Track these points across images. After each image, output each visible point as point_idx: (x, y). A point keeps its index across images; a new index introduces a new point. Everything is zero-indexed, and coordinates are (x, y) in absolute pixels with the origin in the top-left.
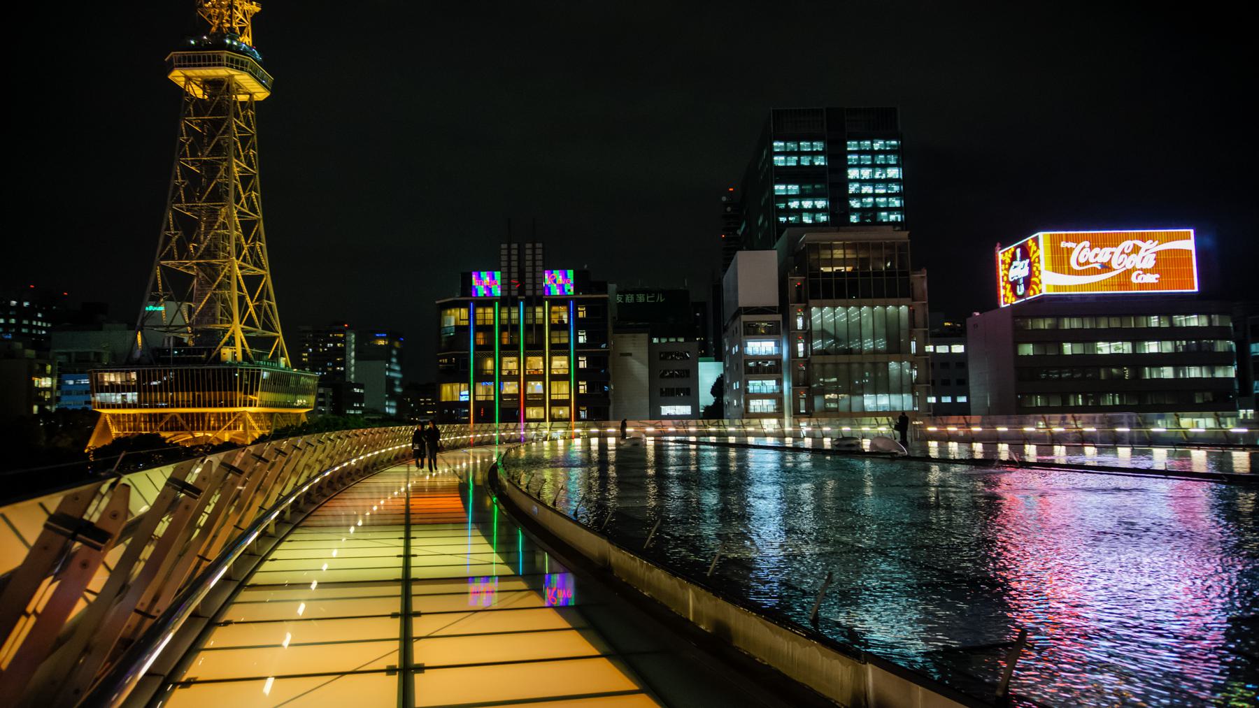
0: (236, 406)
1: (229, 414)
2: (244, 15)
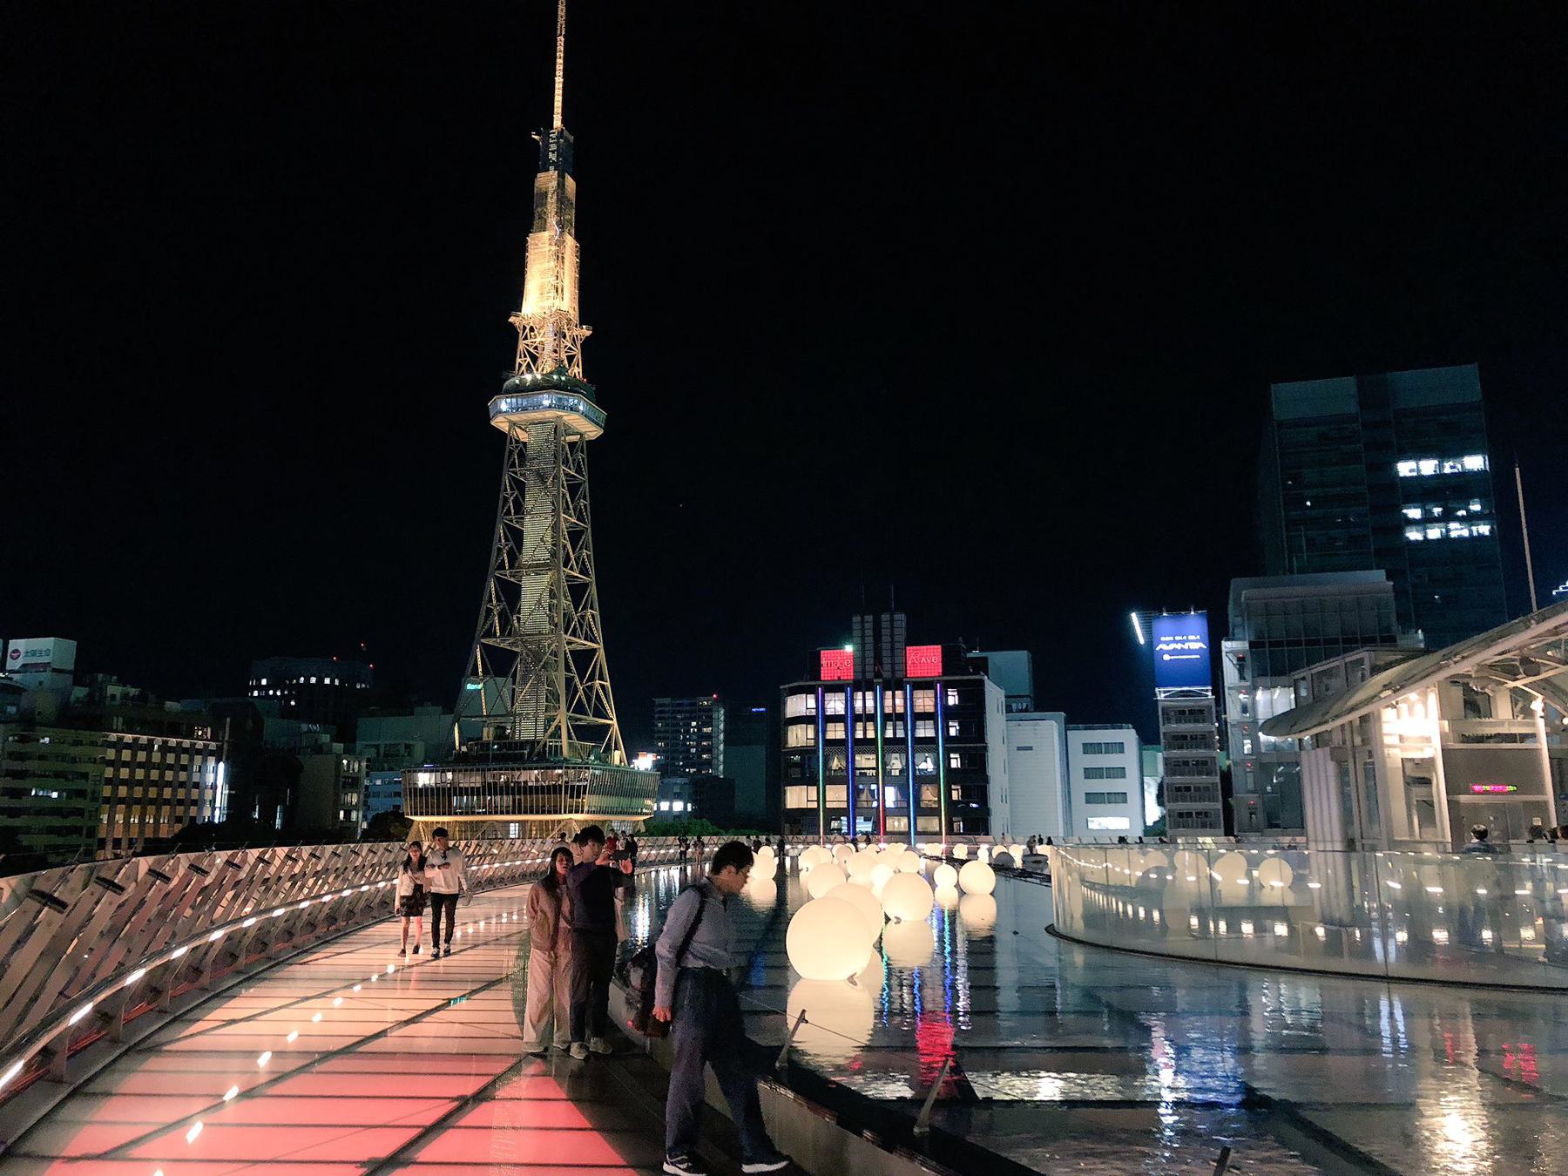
0: (560, 813)
1: (553, 821)
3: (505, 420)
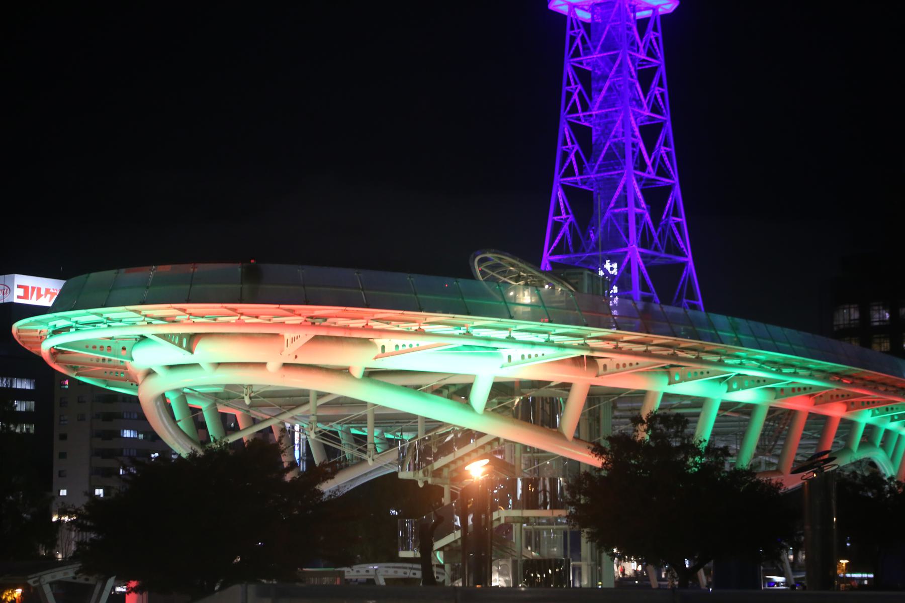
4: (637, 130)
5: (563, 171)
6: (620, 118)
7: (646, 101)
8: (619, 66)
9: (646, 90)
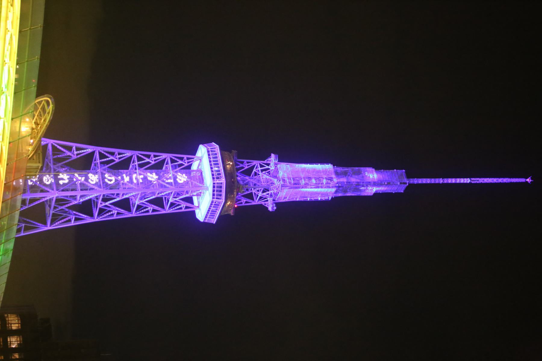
2: (261, 198)
3: (203, 154)
4: (127, 196)
5: (103, 152)
6: (134, 187)
7: (144, 202)
8: (165, 186)
9: (151, 202)
